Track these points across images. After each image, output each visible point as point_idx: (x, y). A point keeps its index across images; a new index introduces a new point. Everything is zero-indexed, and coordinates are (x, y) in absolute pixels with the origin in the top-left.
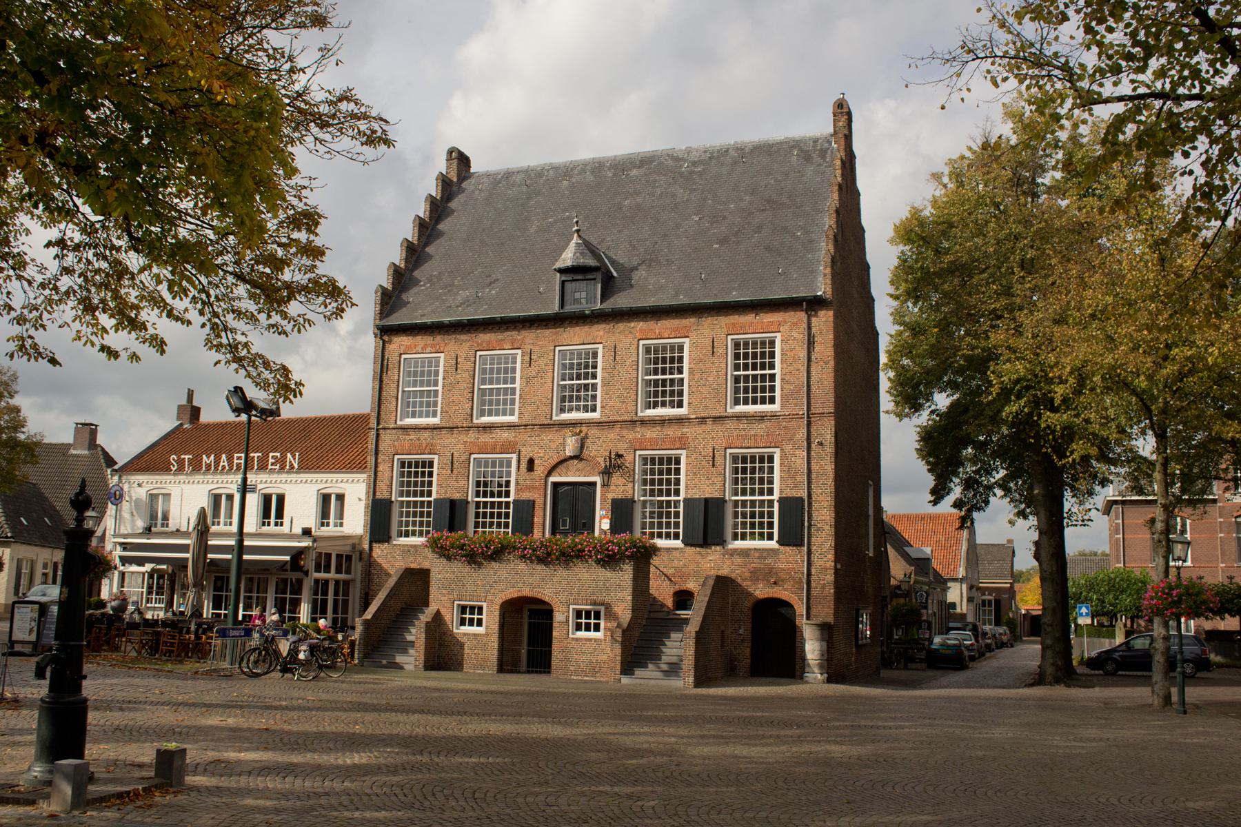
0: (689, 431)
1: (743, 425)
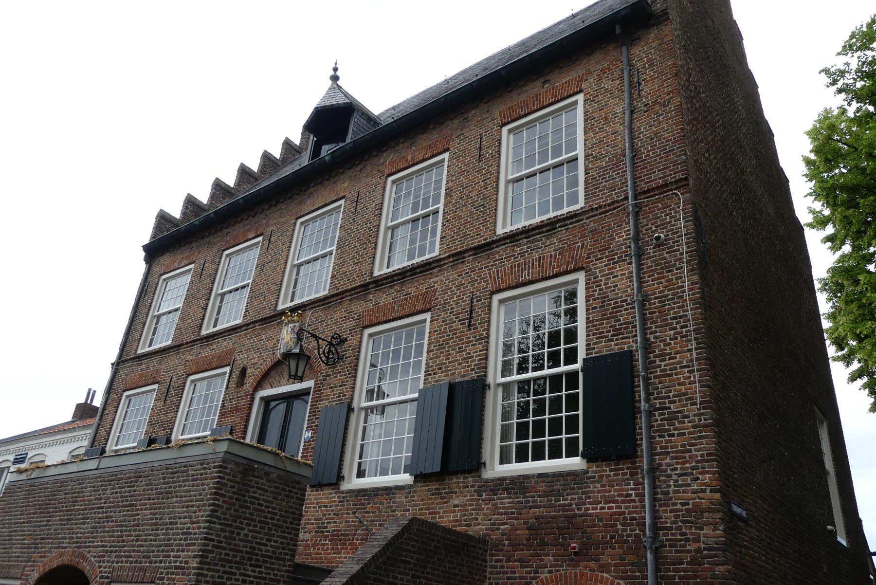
0: (438, 281)
1: (524, 245)
